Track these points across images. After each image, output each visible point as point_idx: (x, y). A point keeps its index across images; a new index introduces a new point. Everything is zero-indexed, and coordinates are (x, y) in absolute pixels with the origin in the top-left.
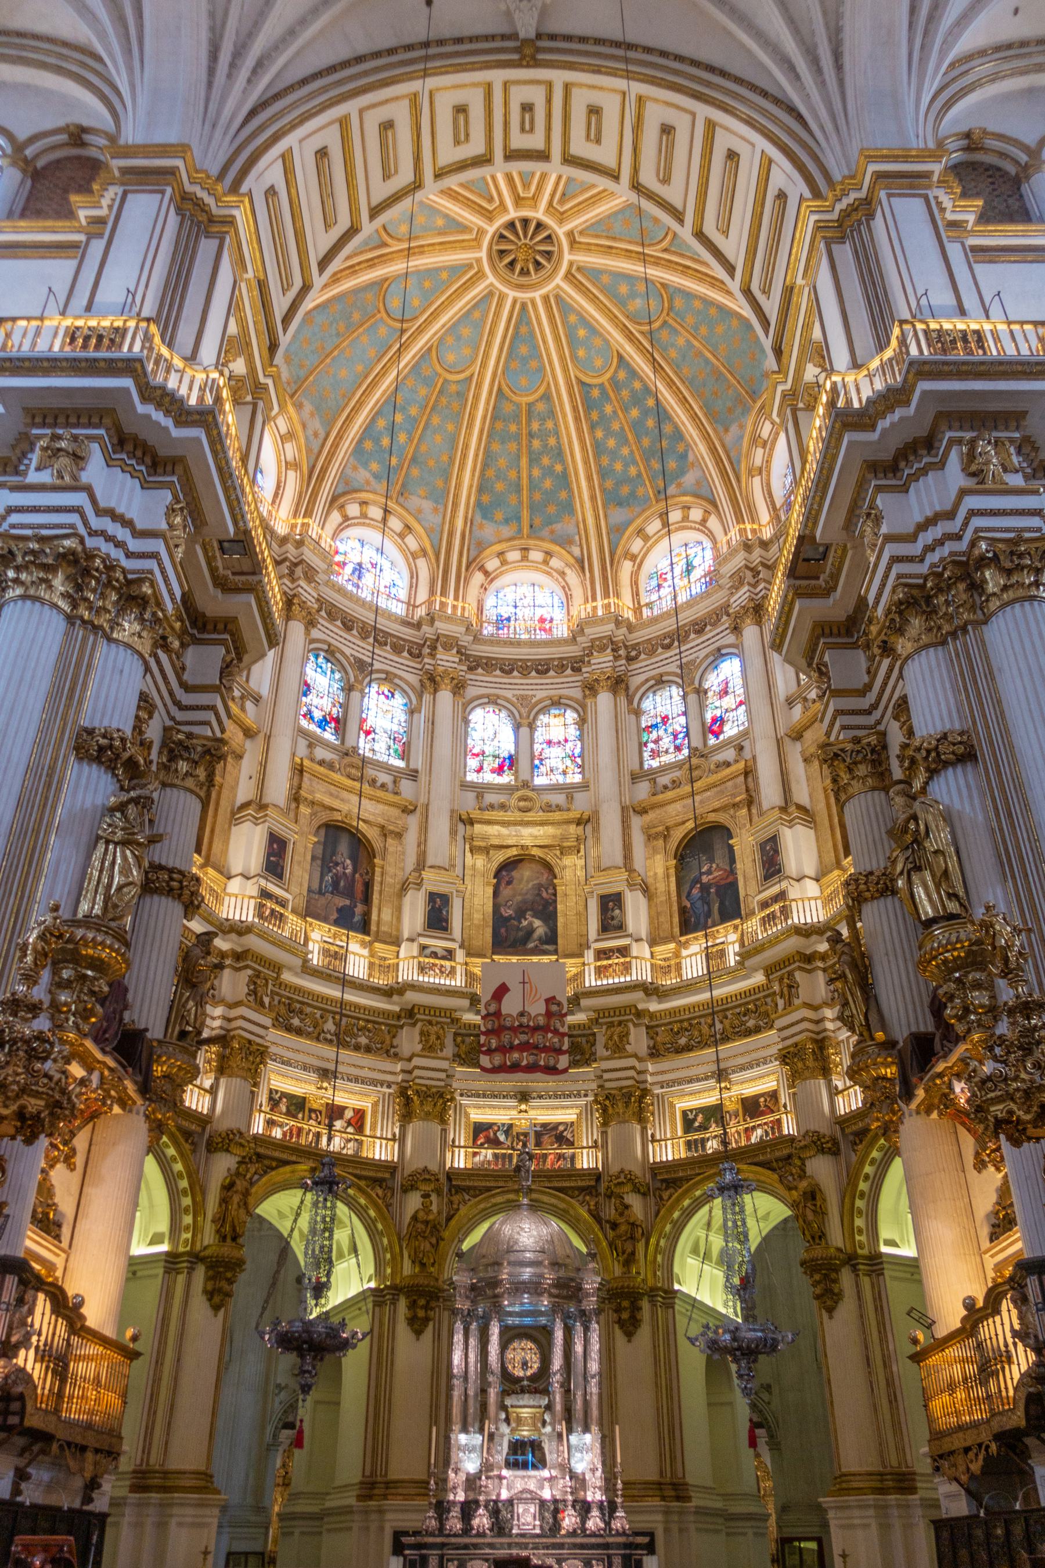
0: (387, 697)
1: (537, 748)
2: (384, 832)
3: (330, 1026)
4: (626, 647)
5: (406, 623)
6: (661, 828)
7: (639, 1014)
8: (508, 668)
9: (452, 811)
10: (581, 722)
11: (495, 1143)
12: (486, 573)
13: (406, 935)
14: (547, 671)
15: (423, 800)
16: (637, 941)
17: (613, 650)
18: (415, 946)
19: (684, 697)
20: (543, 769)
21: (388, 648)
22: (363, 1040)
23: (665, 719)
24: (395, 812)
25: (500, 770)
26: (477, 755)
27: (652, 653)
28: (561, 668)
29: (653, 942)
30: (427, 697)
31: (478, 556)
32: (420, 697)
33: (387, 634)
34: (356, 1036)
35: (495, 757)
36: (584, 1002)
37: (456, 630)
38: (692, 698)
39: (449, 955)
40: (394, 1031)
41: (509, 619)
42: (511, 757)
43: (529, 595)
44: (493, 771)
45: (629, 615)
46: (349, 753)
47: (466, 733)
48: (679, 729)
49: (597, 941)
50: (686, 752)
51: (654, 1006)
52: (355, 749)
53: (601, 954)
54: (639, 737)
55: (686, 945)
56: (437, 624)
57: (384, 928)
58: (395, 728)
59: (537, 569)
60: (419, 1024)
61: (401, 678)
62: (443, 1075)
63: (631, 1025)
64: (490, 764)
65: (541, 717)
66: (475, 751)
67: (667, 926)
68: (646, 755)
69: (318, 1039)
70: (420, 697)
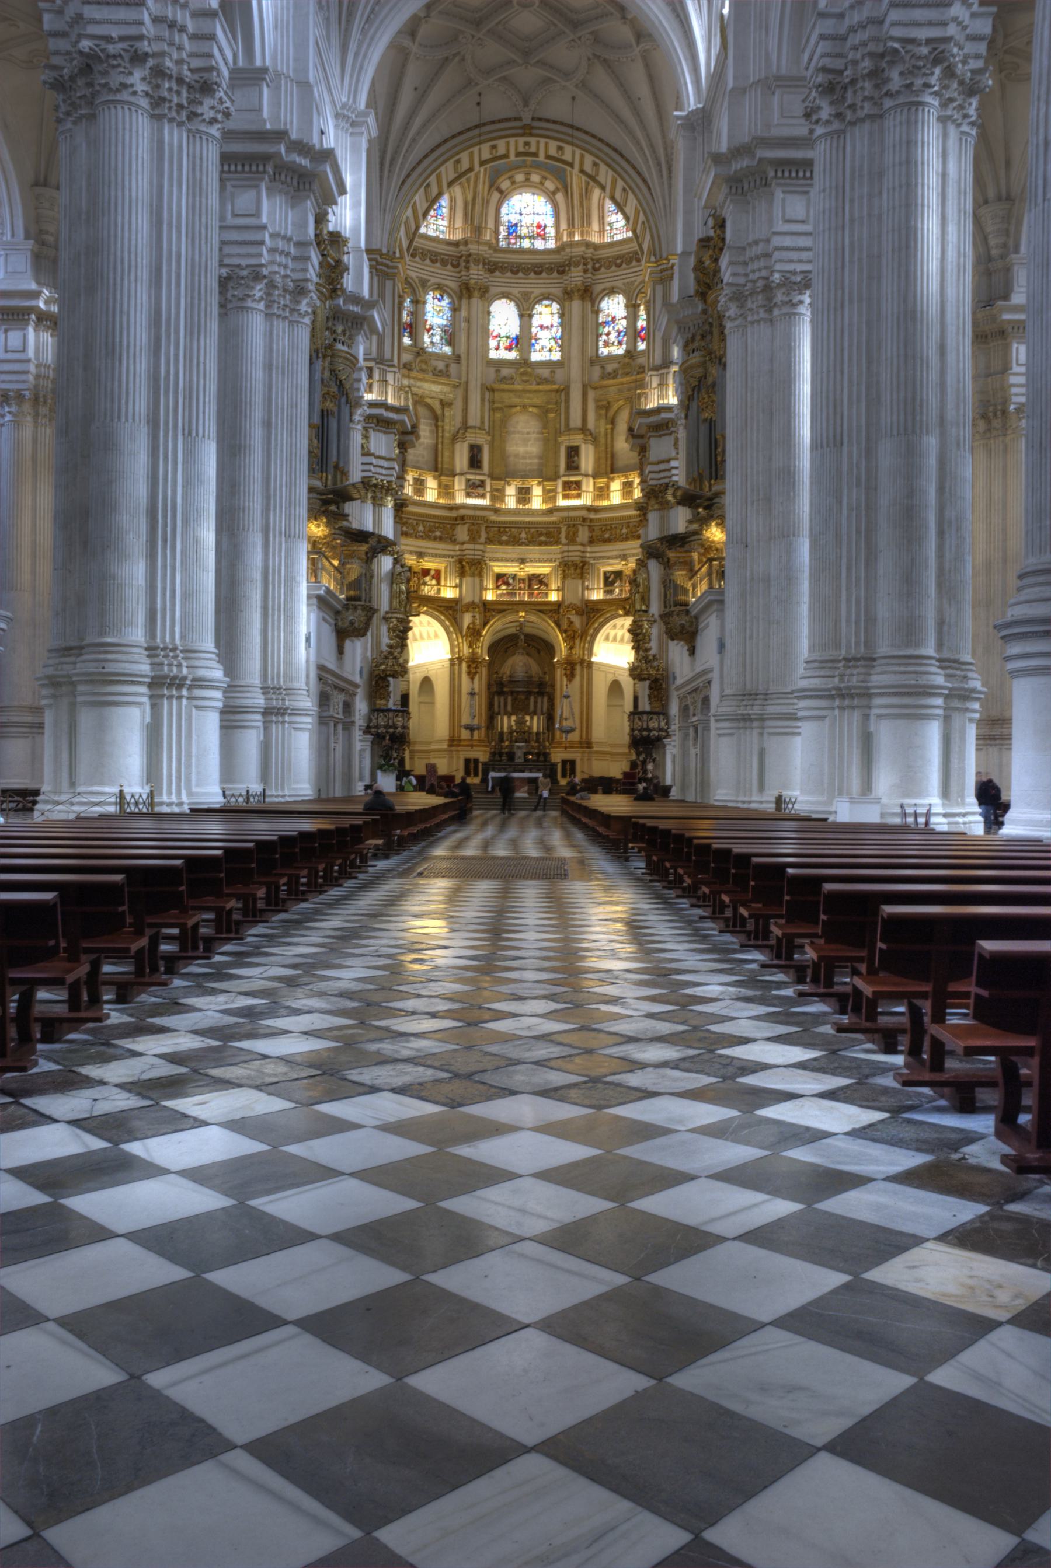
0: (439, 300)
1: (534, 330)
2: (443, 404)
3: (421, 528)
4: (592, 260)
5: (449, 243)
6: (605, 403)
7: (584, 520)
8: (516, 269)
9: (482, 385)
10: (562, 316)
11: (507, 584)
12: (501, 192)
13: (458, 471)
14: (540, 273)
15: (464, 379)
16: (587, 475)
17: (584, 264)
18: (463, 479)
19: (627, 306)
20: (537, 347)
21: (438, 265)
22: (438, 534)
23: (614, 318)
24: (446, 389)
25: (509, 349)
26: (496, 337)
27: (609, 267)
28: (550, 270)
29: (595, 476)
30: (464, 302)
31: (495, 182)
32: (460, 298)
33: (437, 254)
34: (433, 532)
35: (508, 337)
36: (555, 514)
37: (483, 250)
38: (631, 309)
39: (482, 484)
40: (453, 527)
41: (516, 225)
42: (517, 338)
43: (531, 204)
44: (506, 349)
45: (595, 239)
46: (419, 351)
47: (489, 321)
48: (621, 329)
49: (564, 476)
50: (624, 346)
51: (592, 516)
52: (423, 349)
53: (567, 485)
54: (597, 329)
55: (613, 479)
56: (470, 246)
57: (445, 466)
58: (445, 322)
59: (535, 187)
60: (467, 526)
61: (447, 286)
62: (480, 553)
63: (580, 528)
64: (504, 343)
65: (537, 306)
66: (495, 334)
67: (603, 466)
68: (601, 343)
69: (416, 537)
70: (460, 298)
